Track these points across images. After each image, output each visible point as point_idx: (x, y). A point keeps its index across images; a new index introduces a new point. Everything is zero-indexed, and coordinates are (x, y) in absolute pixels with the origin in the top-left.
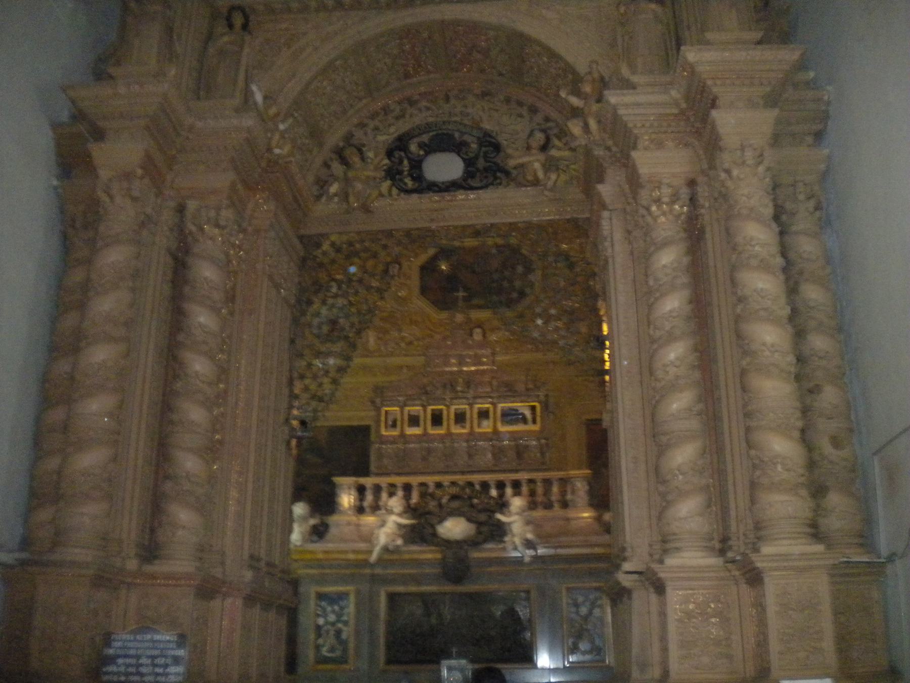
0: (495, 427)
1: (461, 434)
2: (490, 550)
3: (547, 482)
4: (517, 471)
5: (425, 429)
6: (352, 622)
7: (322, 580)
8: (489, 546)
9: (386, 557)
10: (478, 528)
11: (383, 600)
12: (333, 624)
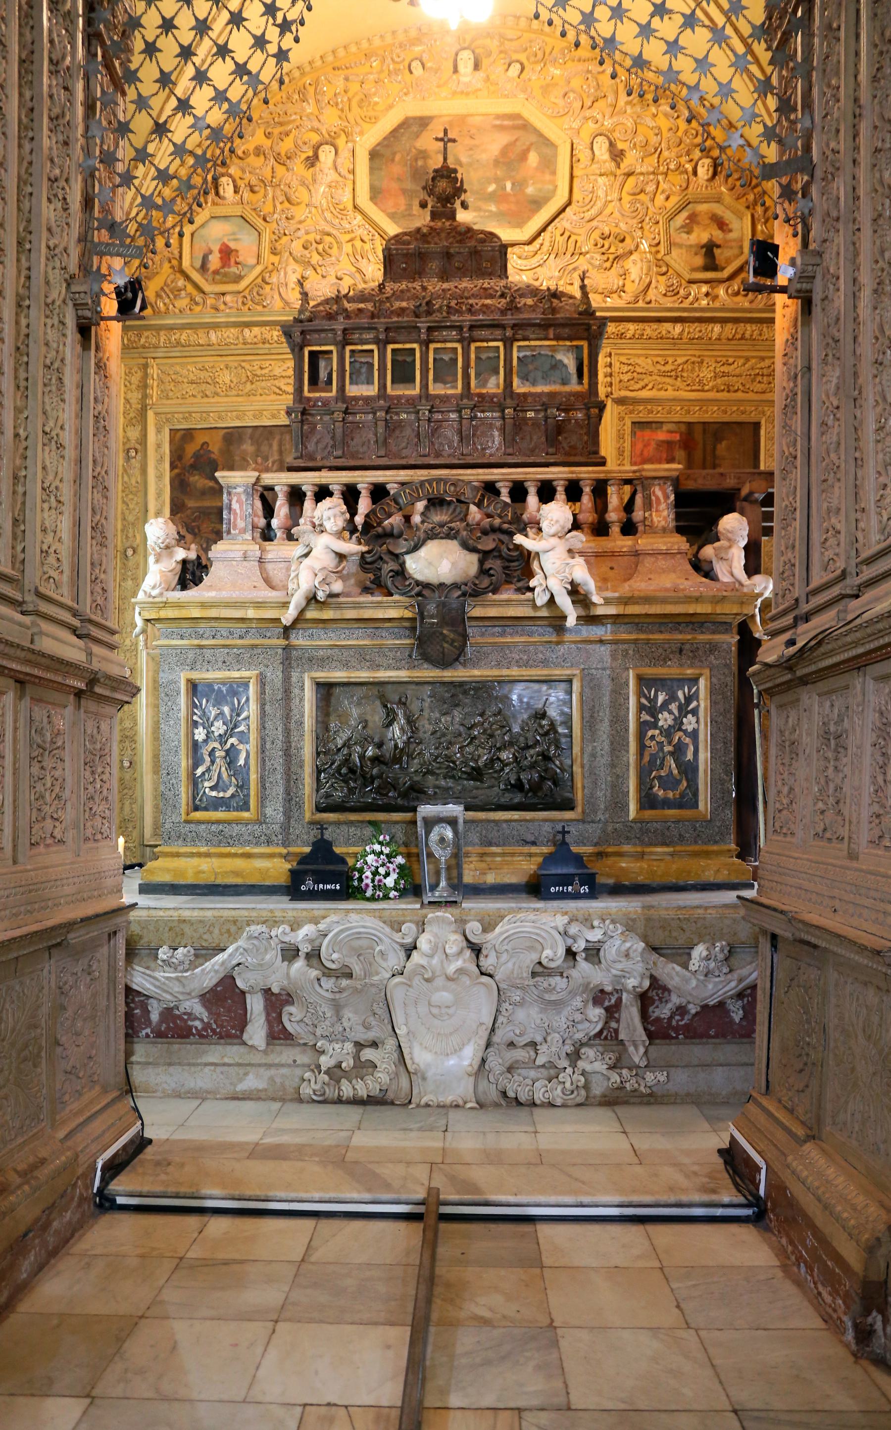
0: (508, 383)
1: (445, 399)
3: (600, 489)
5: (383, 387)
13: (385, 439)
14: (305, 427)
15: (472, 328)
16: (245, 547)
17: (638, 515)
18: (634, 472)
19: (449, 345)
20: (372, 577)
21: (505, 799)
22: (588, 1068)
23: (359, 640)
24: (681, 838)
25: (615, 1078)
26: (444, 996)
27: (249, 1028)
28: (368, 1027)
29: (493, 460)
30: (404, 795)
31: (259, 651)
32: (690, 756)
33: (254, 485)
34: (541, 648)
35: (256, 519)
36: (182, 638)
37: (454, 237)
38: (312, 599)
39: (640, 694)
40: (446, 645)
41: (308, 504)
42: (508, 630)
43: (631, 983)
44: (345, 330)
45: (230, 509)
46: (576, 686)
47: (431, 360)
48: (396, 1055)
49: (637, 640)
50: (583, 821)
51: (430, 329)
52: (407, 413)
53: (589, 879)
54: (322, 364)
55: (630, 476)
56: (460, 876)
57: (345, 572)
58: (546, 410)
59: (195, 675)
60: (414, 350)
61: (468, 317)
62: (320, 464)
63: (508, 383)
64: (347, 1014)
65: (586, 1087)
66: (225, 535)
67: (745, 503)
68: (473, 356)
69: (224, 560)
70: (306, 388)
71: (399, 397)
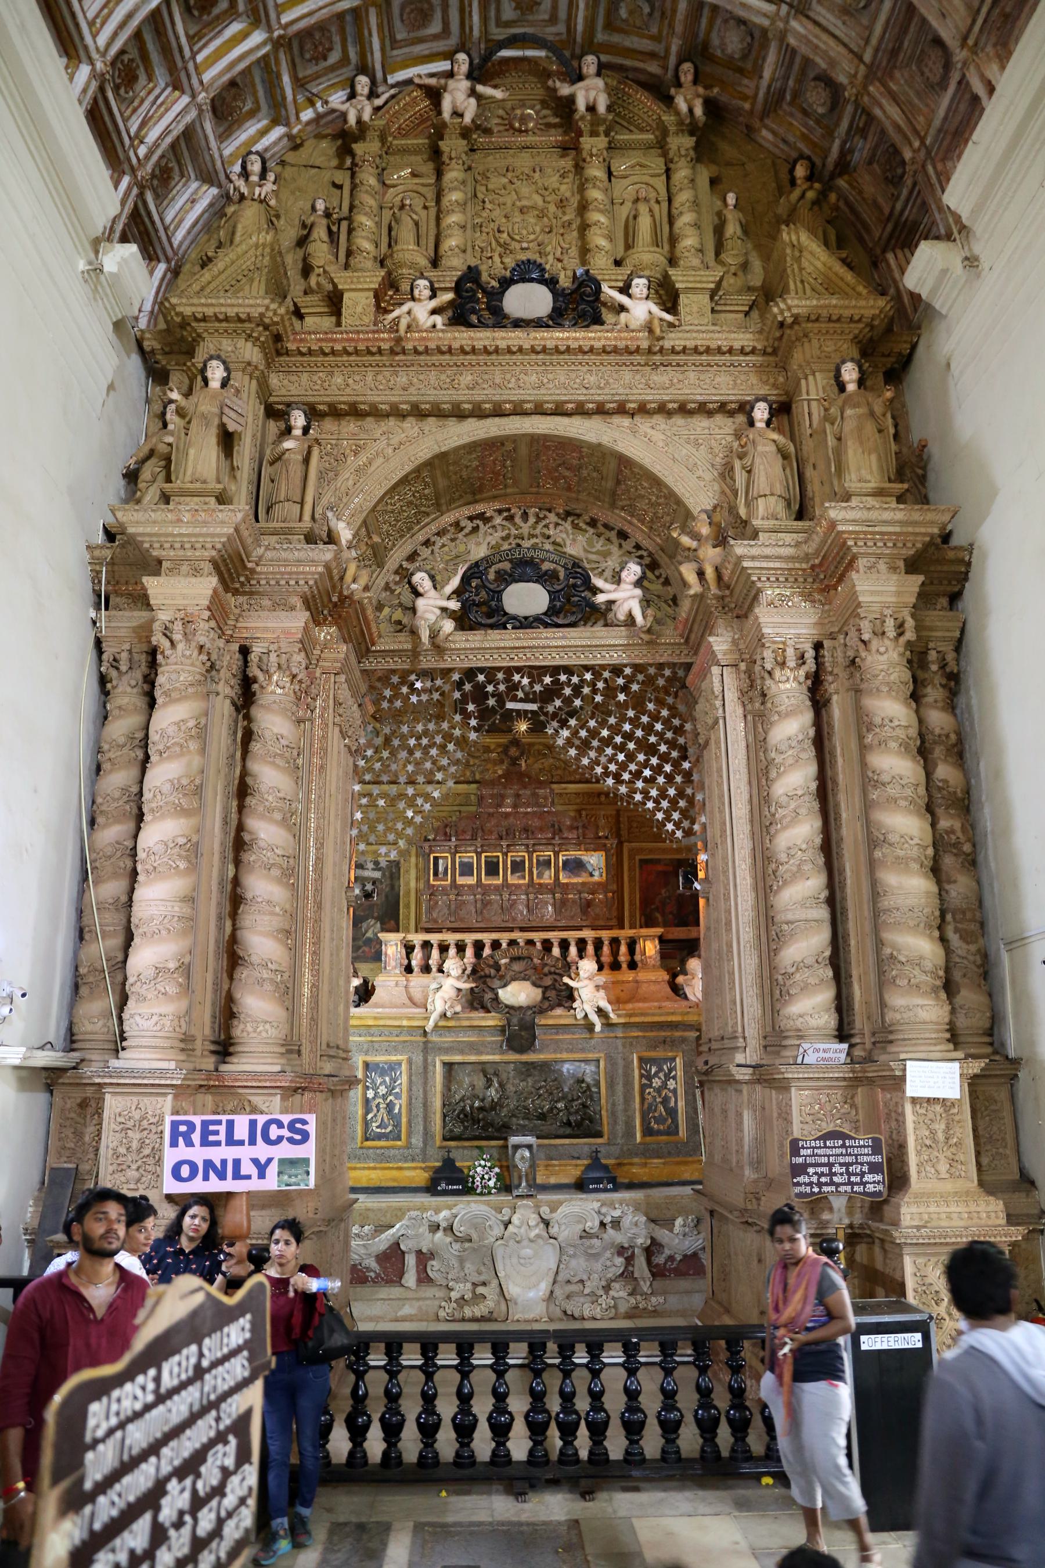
1: (518, 886)
2: (558, 1015)
3: (615, 942)
4: (579, 928)
6: (404, 1096)
7: (371, 1048)
8: (559, 1011)
9: (442, 1023)
10: (544, 993)
11: (439, 1068)
12: (384, 1097)
17: (638, 957)
21: (561, 1131)
22: (616, 1295)
23: (472, 1038)
24: (669, 1153)
25: (633, 1301)
26: (528, 1252)
27: (406, 1276)
28: (480, 1273)
30: (498, 1130)
32: (672, 1104)
39: (641, 1068)
43: (640, 1241)
46: (602, 1064)
48: (498, 1290)
50: (608, 1144)
53: (613, 1180)
54: (441, 861)
56: (535, 1179)
59: (369, 1059)
64: (468, 1265)
65: (615, 1307)
71: (490, 885)
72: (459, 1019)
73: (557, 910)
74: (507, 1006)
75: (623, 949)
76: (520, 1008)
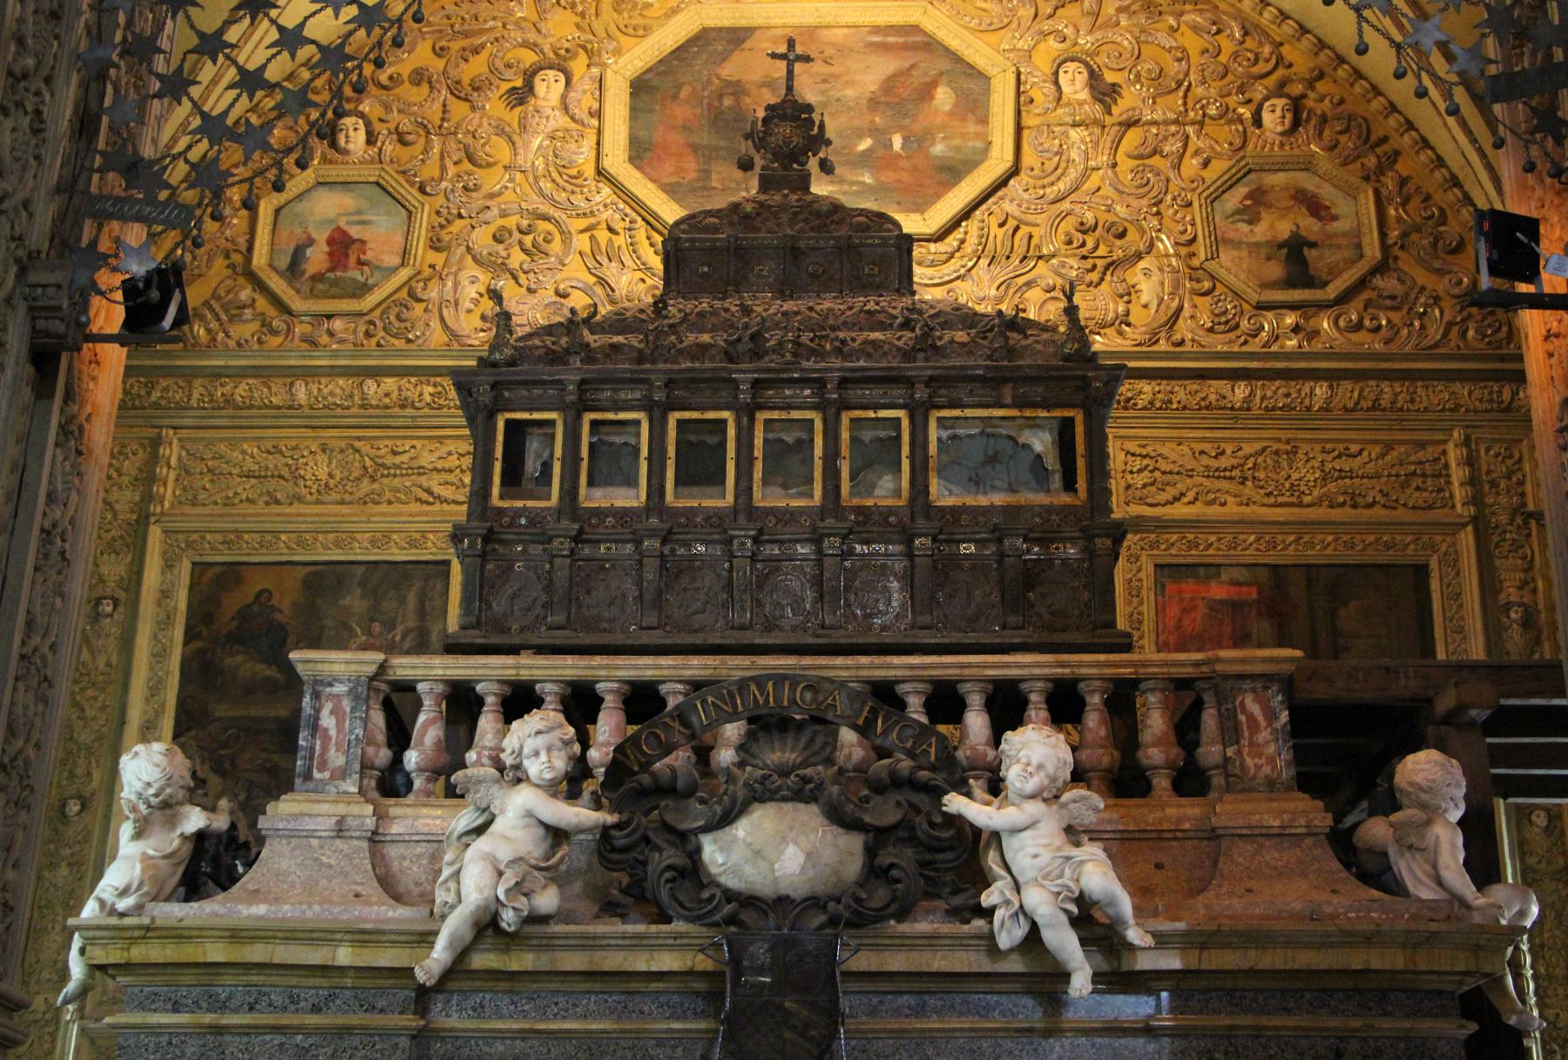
0: (919, 487)
1: (786, 517)
3: (1122, 698)
5: (656, 490)
10: (870, 852)
13: (659, 594)
14: (490, 567)
15: (844, 383)
16: (341, 809)
18: (1197, 664)
19: (796, 415)
20: (625, 881)
29: (888, 638)
31: (356, 1041)
33: (372, 679)
34: (1008, 1044)
35: (370, 750)
36: (176, 1010)
37: (805, 220)
38: (487, 926)
40: (788, 1035)
41: (487, 723)
42: (932, 1001)
44: (583, 382)
45: (315, 726)
47: (758, 442)
49: (1232, 1028)
51: (756, 384)
52: (706, 543)
54: (533, 445)
55: (1188, 671)
57: (563, 867)
58: (1000, 541)
60: (724, 422)
61: (837, 363)
62: (516, 640)
63: (919, 487)
66: (298, 781)
67: (1444, 728)
68: (845, 436)
69: (291, 835)
70: (496, 491)
71: (690, 513)
72: (548, 944)
73: (922, 597)
74: (730, 895)
75: (1155, 721)
76: (783, 901)
